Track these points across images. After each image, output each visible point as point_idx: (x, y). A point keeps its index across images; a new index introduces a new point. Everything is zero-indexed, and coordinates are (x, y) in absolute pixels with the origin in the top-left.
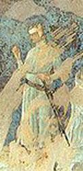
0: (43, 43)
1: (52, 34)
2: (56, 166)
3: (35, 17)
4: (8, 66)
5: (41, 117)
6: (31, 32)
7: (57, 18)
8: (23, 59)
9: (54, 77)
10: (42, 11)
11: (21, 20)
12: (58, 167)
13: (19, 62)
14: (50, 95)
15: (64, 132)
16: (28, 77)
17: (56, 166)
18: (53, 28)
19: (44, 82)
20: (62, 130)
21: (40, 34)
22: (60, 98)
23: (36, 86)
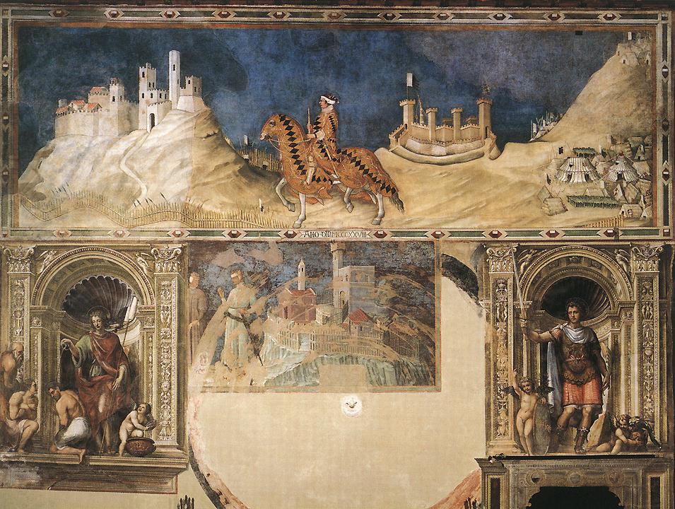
0: (241, 284)
1: (249, 278)
2: (252, 381)
3: (235, 264)
4: (214, 302)
5: (240, 343)
6: (232, 276)
7: (253, 266)
8: (226, 297)
9: (251, 311)
10: (241, 260)
11: (225, 267)
12: (253, 383)
13: (223, 300)
14: (247, 326)
15: (259, 355)
16: (230, 311)
17: (252, 381)
18: (250, 273)
19: (242, 316)
20: (257, 353)
21: (240, 277)
22: (255, 328)
23: (237, 318)
